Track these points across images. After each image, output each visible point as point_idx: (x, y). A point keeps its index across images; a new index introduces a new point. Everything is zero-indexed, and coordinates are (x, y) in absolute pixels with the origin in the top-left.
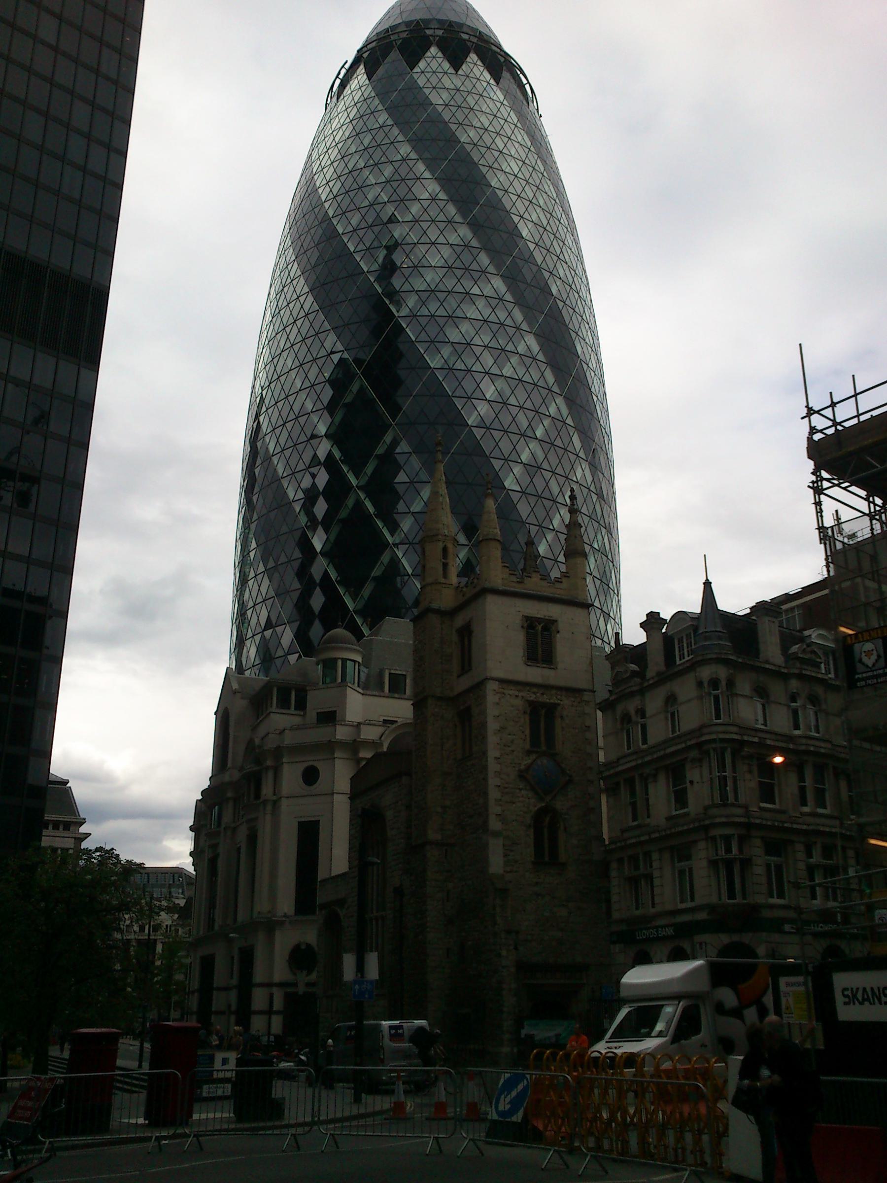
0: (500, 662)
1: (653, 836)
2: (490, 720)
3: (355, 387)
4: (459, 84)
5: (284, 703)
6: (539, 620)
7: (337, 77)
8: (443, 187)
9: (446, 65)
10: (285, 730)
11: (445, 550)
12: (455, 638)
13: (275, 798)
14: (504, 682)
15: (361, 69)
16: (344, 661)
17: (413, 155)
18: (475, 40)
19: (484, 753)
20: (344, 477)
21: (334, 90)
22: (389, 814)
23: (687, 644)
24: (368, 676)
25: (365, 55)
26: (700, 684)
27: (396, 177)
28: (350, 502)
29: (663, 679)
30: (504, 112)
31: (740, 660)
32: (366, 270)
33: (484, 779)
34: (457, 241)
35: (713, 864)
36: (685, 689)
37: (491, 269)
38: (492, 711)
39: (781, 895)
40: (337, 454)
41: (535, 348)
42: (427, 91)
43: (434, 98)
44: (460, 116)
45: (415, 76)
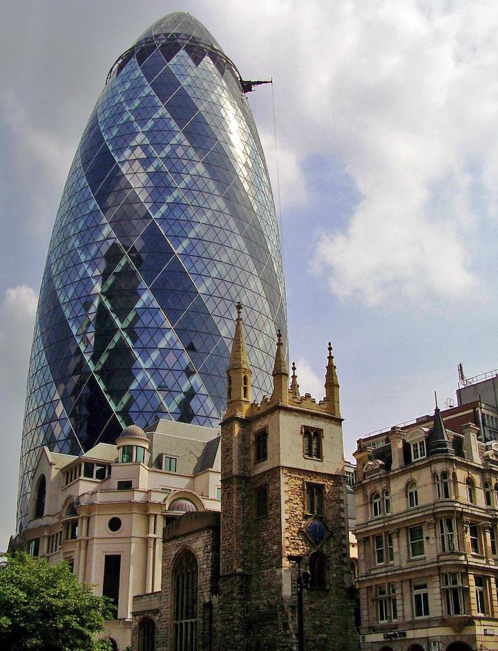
1: (397, 572)
2: (282, 493)
3: (123, 262)
4: (198, 74)
5: (89, 473)
6: (312, 429)
7: (117, 62)
9: (190, 62)
10: (97, 492)
11: (245, 378)
12: (252, 438)
13: (87, 538)
14: (291, 470)
15: (134, 60)
16: (137, 446)
17: (168, 116)
18: (209, 48)
19: (279, 516)
20: (113, 322)
21: (113, 70)
22: (200, 555)
23: (421, 448)
24: (151, 458)
26: (434, 475)
27: (156, 129)
28: (116, 338)
29: (404, 473)
31: (460, 460)
33: (278, 533)
35: (445, 592)
36: (423, 478)
37: (216, 192)
38: (284, 488)
39: (483, 612)
40: (108, 306)
41: (243, 245)
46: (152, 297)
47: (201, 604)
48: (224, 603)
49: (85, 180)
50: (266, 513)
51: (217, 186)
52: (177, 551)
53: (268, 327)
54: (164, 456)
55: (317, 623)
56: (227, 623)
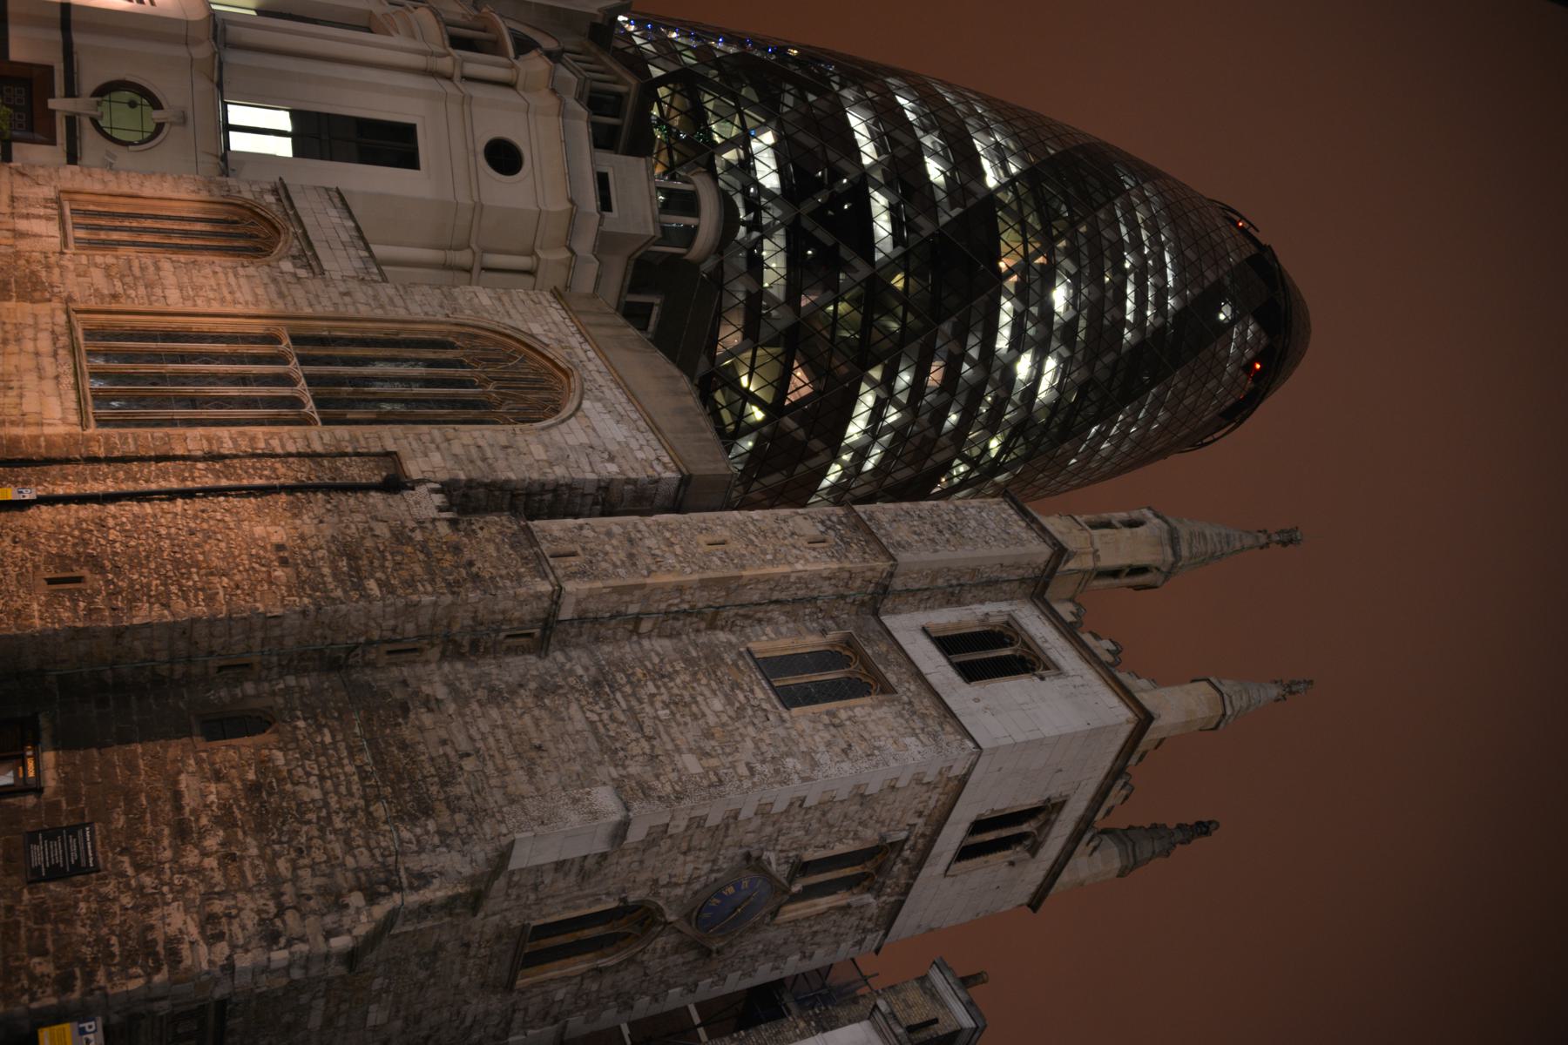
0: (1000, 770)
47: (391, 446)
48: (424, 548)
50: (791, 698)
52: (546, 340)
54: (657, 301)
55: (377, 984)
56: (343, 564)
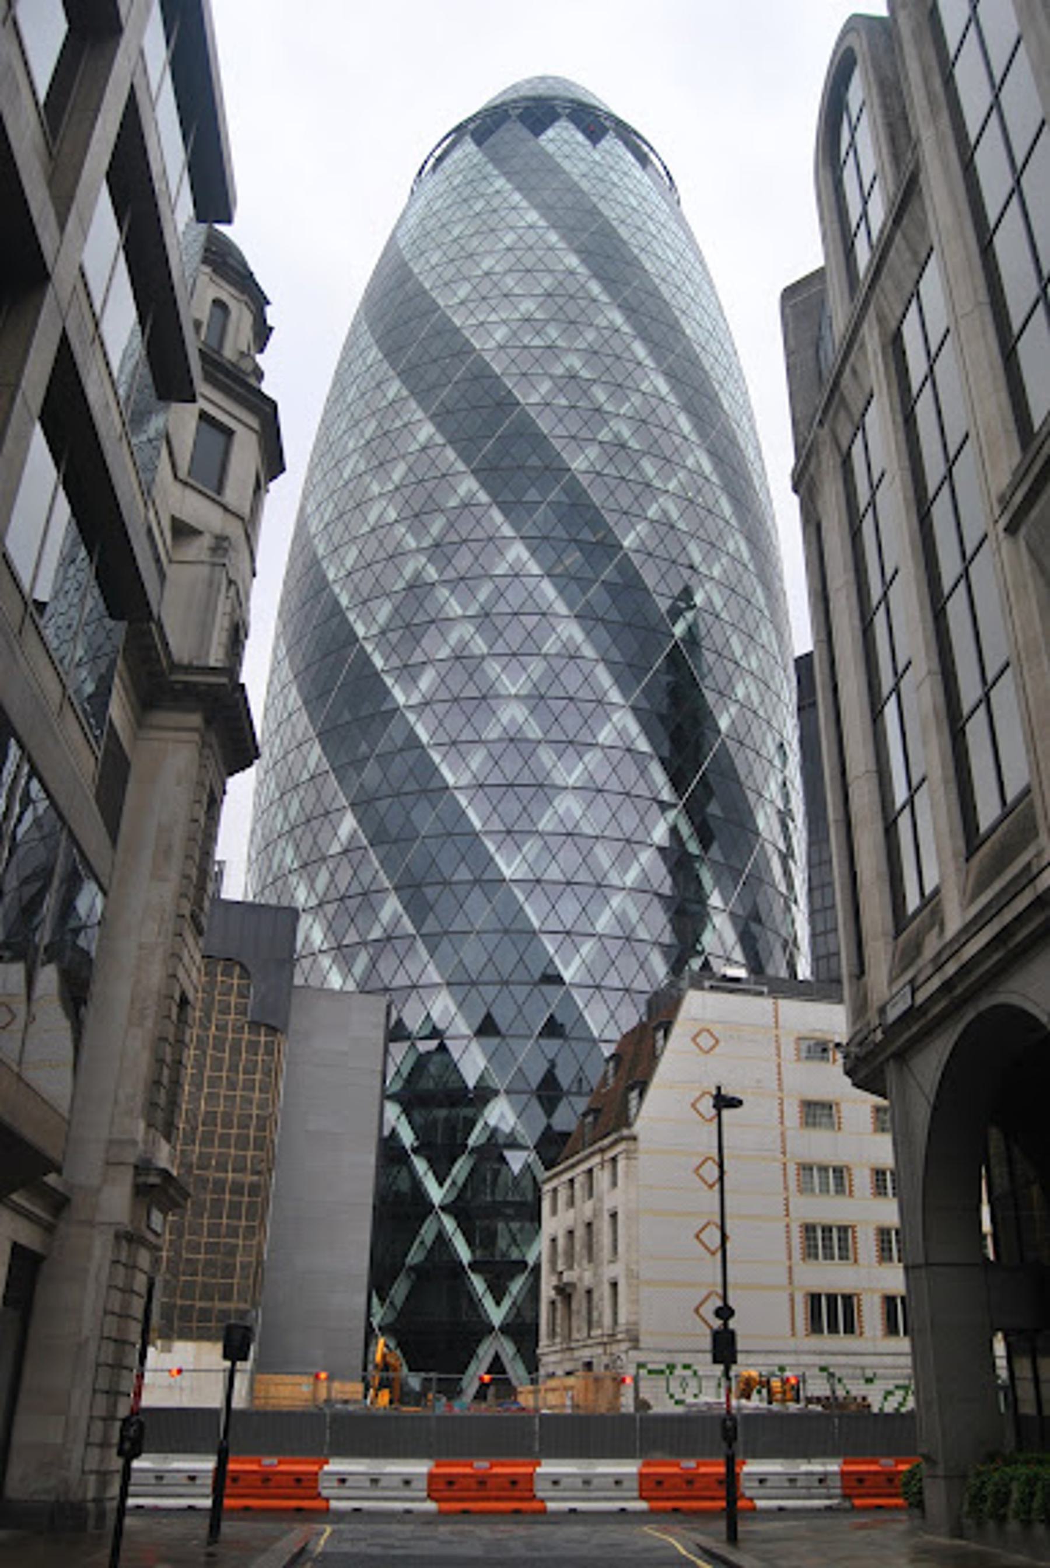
4: (598, 158)
8: (583, 261)
9: (580, 137)
25: (472, 126)
30: (655, 198)
32: (478, 347)
34: (605, 323)
42: (559, 160)
43: (566, 165)
44: (601, 189)
45: (543, 143)
46: (525, 555)
49: (375, 349)
51: (651, 353)
53: (764, 633)
